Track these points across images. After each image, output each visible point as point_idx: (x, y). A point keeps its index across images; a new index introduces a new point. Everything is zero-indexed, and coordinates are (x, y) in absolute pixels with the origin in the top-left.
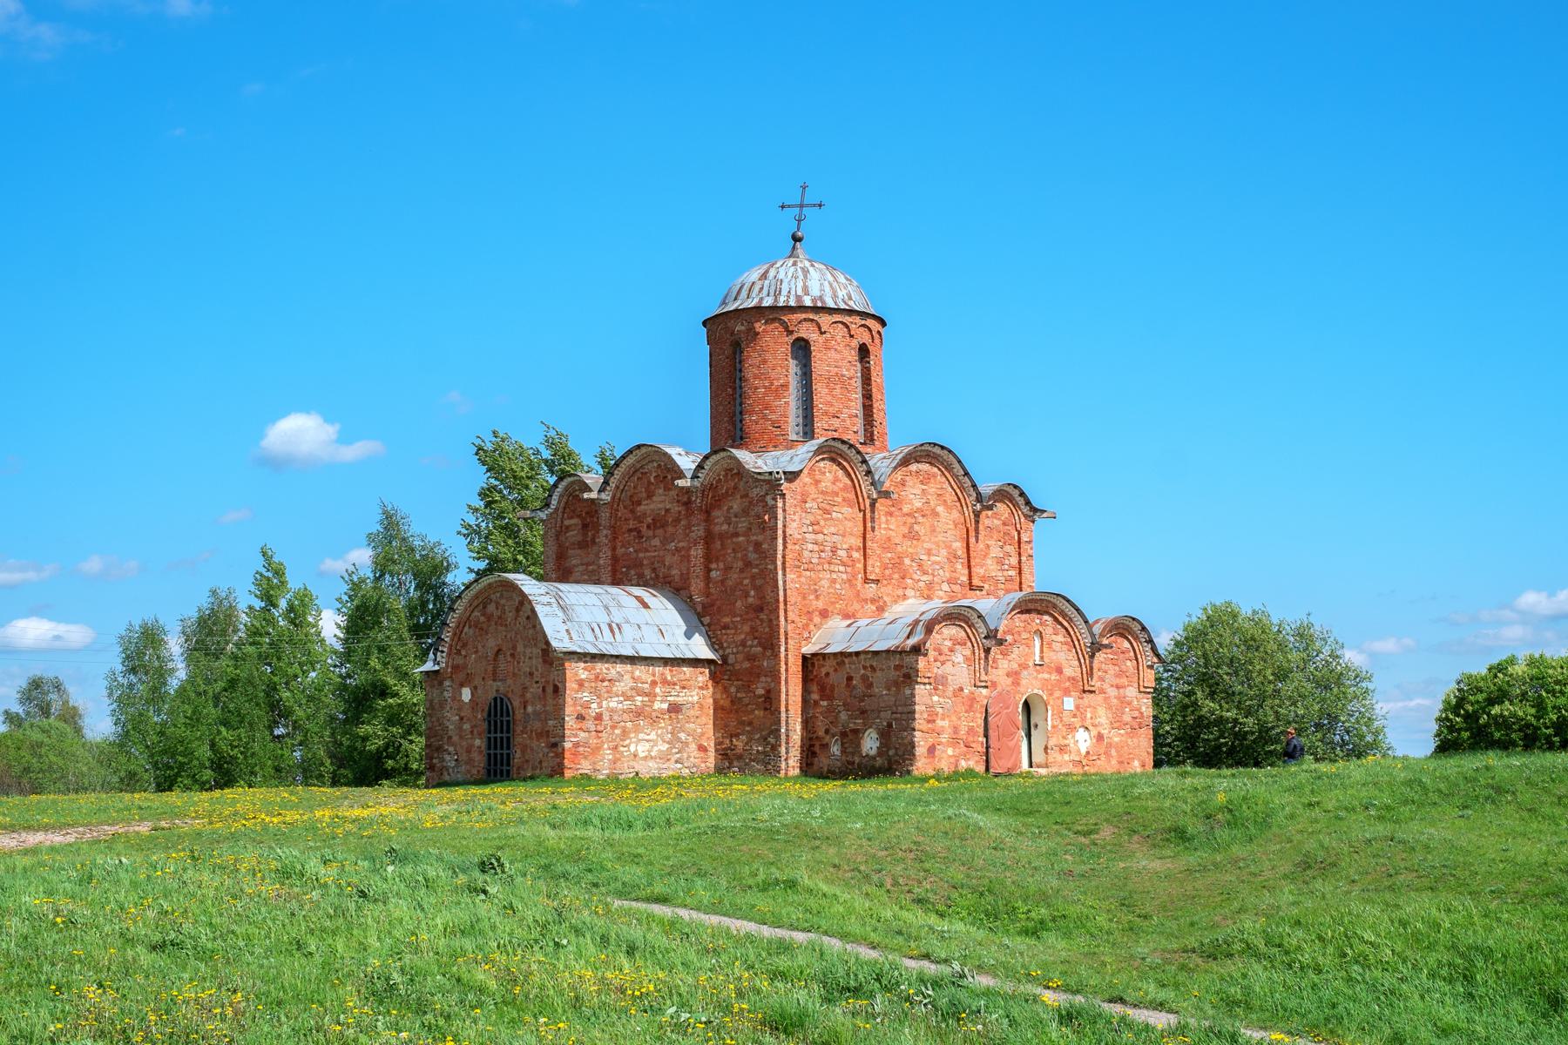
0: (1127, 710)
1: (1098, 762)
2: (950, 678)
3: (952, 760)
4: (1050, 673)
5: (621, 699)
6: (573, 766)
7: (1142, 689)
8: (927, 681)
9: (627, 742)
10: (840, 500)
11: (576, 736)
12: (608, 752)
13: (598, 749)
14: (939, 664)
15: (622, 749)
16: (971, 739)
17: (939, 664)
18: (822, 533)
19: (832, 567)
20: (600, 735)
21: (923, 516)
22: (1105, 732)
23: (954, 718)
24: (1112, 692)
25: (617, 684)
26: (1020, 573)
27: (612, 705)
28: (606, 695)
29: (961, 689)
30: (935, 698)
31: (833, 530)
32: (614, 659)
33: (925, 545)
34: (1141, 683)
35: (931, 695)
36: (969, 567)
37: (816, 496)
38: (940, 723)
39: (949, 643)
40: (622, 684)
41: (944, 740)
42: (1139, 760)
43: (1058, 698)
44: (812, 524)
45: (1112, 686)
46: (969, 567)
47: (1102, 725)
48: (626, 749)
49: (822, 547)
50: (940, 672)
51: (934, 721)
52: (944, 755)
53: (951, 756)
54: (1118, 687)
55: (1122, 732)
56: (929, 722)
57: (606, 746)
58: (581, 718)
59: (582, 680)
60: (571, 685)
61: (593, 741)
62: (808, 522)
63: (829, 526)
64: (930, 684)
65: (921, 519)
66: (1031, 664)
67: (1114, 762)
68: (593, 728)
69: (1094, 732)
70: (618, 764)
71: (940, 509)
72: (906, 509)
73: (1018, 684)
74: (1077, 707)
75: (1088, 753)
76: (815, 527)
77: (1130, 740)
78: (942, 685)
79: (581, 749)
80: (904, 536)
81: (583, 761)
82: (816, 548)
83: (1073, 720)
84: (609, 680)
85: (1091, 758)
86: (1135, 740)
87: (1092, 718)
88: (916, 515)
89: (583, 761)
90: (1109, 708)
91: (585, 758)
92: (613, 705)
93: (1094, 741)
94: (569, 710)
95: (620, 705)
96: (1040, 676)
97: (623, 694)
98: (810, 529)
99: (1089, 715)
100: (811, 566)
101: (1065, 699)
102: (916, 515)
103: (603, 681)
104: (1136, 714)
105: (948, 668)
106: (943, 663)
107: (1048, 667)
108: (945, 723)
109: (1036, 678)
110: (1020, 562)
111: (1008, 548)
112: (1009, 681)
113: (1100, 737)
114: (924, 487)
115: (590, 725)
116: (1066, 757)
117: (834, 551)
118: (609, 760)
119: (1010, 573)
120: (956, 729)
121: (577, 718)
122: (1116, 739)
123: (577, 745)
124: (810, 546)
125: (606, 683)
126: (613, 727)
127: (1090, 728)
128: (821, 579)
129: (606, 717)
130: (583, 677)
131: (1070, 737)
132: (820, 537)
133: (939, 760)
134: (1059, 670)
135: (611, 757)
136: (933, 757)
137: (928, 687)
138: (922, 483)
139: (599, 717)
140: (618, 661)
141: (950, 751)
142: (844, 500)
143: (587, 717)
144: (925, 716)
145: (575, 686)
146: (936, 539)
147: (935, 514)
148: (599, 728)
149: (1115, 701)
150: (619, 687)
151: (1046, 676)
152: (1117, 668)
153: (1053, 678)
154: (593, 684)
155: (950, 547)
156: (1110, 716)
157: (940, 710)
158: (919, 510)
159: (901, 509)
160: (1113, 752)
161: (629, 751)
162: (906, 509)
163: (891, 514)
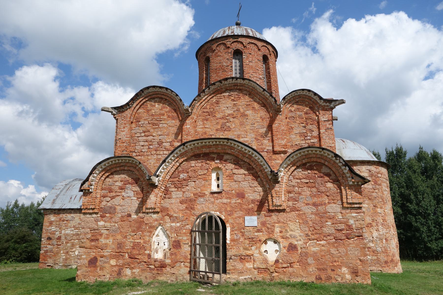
0: (329, 223)
1: (290, 269)
2: (118, 208)
3: (116, 269)
4: (230, 198)
5: (73, 229)
6: (43, 261)
7: (345, 205)
8: (91, 211)
9: (74, 250)
10: (165, 117)
11: (46, 247)
12: (63, 255)
13: (58, 253)
14: (108, 199)
15: (71, 253)
16: (135, 252)
17: (108, 199)
18: (152, 136)
19: (158, 152)
20: (59, 246)
21: (233, 118)
22: (299, 244)
23: (119, 237)
24: (308, 210)
25: (71, 222)
26: (320, 140)
27: (67, 232)
28: (64, 228)
29: (129, 215)
30: (101, 223)
31: (159, 133)
32: (70, 211)
33: (235, 133)
34: (345, 200)
35: (97, 221)
36: (273, 141)
37: (147, 118)
38: (103, 241)
39: (119, 184)
40: (74, 222)
41: (106, 254)
42: (349, 267)
43: (239, 217)
44: (144, 132)
45: (307, 204)
46: (273, 141)
47: (295, 237)
48: (73, 253)
49: (150, 143)
50: (109, 204)
51: (98, 240)
52: (107, 265)
53: (112, 266)
54: (314, 205)
55: (322, 242)
56: (92, 240)
57: (62, 252)
58: (49, 239)
59: (51, 221)
60: (46, 224)
61: (55, 250)
62: (142, 131)
63: (157, 132)
64: (96, 213)
65: (232, 120)
66: (207, 193)
67: (312, 269)
68: (55, 243)
69: (285, 243)
70: (68, 261)
71: (249, 112)
72: (218, 116)
73: (193, 209)
74: (263, 224)
75: (277, 261)
76: (146, 133)
77: (333, 251)
78: (110, 213)
79: (49, 253)
80: (217, 130)
81: (49, 259)
82: (146, 143)
83: (256, 234)
84: (67, 221)
85: (280, 266)
86: (342, 249)
87: (281, 232)
88: (228, 118)
89: (49, 259)
90: (305, 222)
91: (50, 258)
92: (68, 232)
93: (285, 251)
94: (43, 235)
95: (72, 232)
96: (218, 201)
97: (74, 227)
98: (143, 134)
99: (277, 230)
100: (142, 153)
101: (247, 218)
102: (228, 118)
103: (63, 221)
104: (342, 226)
105: (117, 201)
106: (113, 198)
107: (227, 193)
108: (110, 241)
109: (213, 203)
110: (320, 133)
111: (310, 127)
112: (184, 206)
113: (292, 248)
114: (235, 102)
115: (54, 242)
116: (249, 265)
117: (160, 143)
118: (63, 259)
119: (312, 141)
120: (120, 245)
121: (47, 239)
122: (313, 249)
123: (46, 252)
124: (142, 143)
125: (65, 222)
126: (67, 243)
127: (281, 240)
128: (149, 159)
129: (63, 238)
130: (52, 220)
131: (253, 248)
132: (150, 138)
133: (102, 269)
134: (241, 195)
135: (64, 257)
136: (95, 267)
137: (94, 216)
138: (233, 100)
139: (59, 238)
140: (72, 212)
141: (113, 262)
142: (169, 117)
143: (53, 238)
144: (89, 236)
145: (48, 224)
146: (245, 129)
147: (244, 115)
148: (59, 243)
149: (313, 216)
150: (72, 224)
151: (225, 201)
152: (314, 190)
153: (233, 201)
154: (58, 223)
155: (257, 132)
156: (307, 229)
157: (106, 232)
158: (229, 115)
159: (215, 116)
160: (310, 260)
161: (75, 254)
162: (218, 116)
163: (207, 120)
